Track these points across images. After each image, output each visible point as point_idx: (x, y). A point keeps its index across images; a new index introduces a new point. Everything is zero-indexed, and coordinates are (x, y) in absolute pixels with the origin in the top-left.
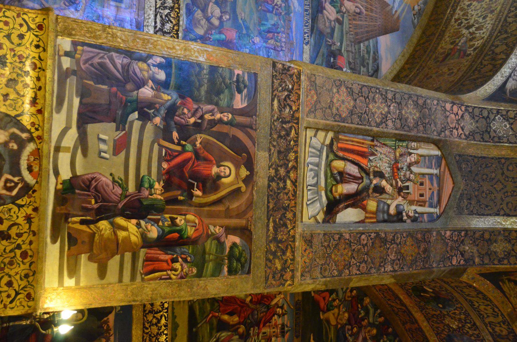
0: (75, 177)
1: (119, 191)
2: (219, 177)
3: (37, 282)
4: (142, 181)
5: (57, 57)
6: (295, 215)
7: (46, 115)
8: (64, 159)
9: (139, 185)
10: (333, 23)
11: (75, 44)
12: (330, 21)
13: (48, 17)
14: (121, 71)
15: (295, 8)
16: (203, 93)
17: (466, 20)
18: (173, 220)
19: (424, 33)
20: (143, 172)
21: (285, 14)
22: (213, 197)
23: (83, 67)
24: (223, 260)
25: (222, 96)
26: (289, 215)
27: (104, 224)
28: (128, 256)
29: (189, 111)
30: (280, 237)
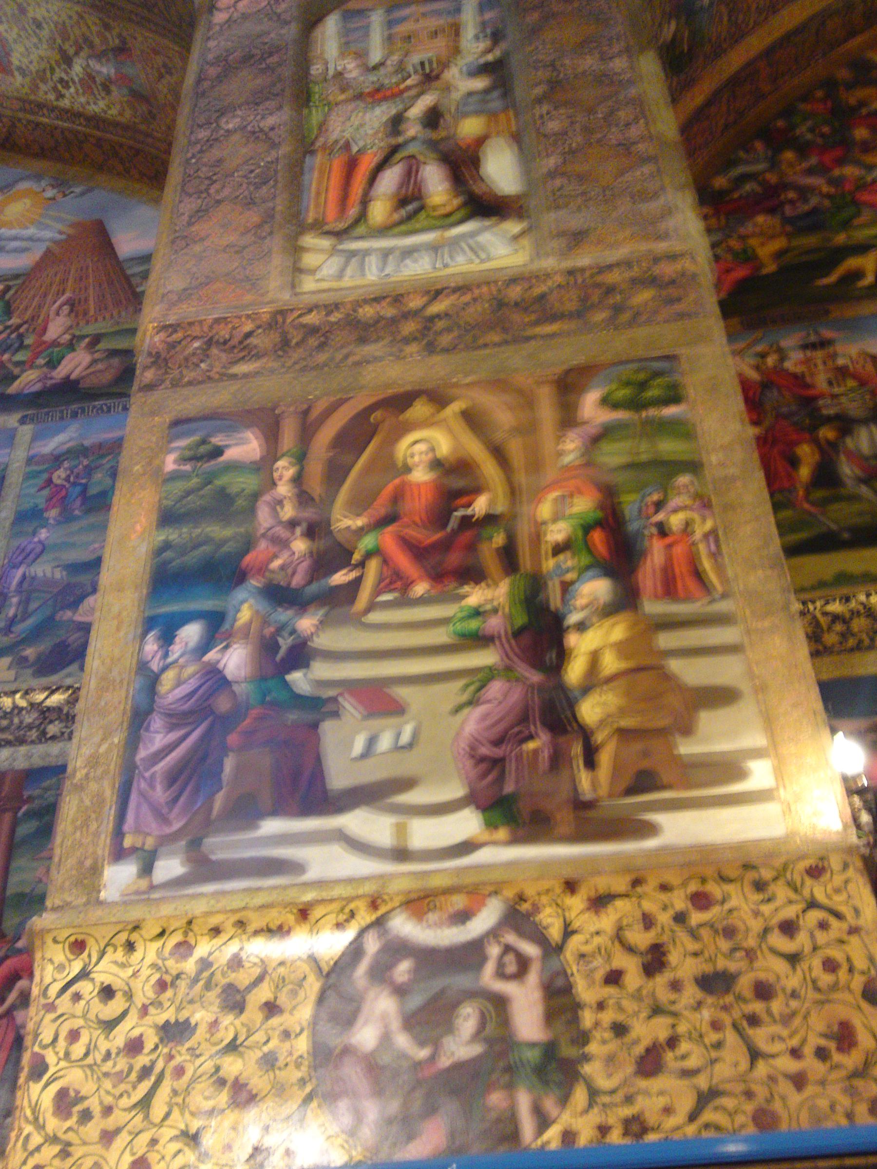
0: (472, 799)
1: (496, 688)
2: (437, 464)
3: (771, 855)
4: (464, 636)
5: (155, 895)
6: (513, 281)
7: (309, 896)
8: (426, 833)
9: (479, 640)
10: (97, 356)
11: (119, 854)
12: (94, 362)
13: (49, 931)
14: (182, 732)
15: (71, 440)
16: (228, 532)
17: (52, 69)
18: (558, 549)
19: (100, 168)
20: (440, 636)
21: (86, 456)
22: (489, 469)
23: (177, 825)
24: (648, 422)
25: (233, 490)
26: (515, 293)
27: (590, 711)
28: (665, 640)
29: (275, 556)
30: (571, 306)
